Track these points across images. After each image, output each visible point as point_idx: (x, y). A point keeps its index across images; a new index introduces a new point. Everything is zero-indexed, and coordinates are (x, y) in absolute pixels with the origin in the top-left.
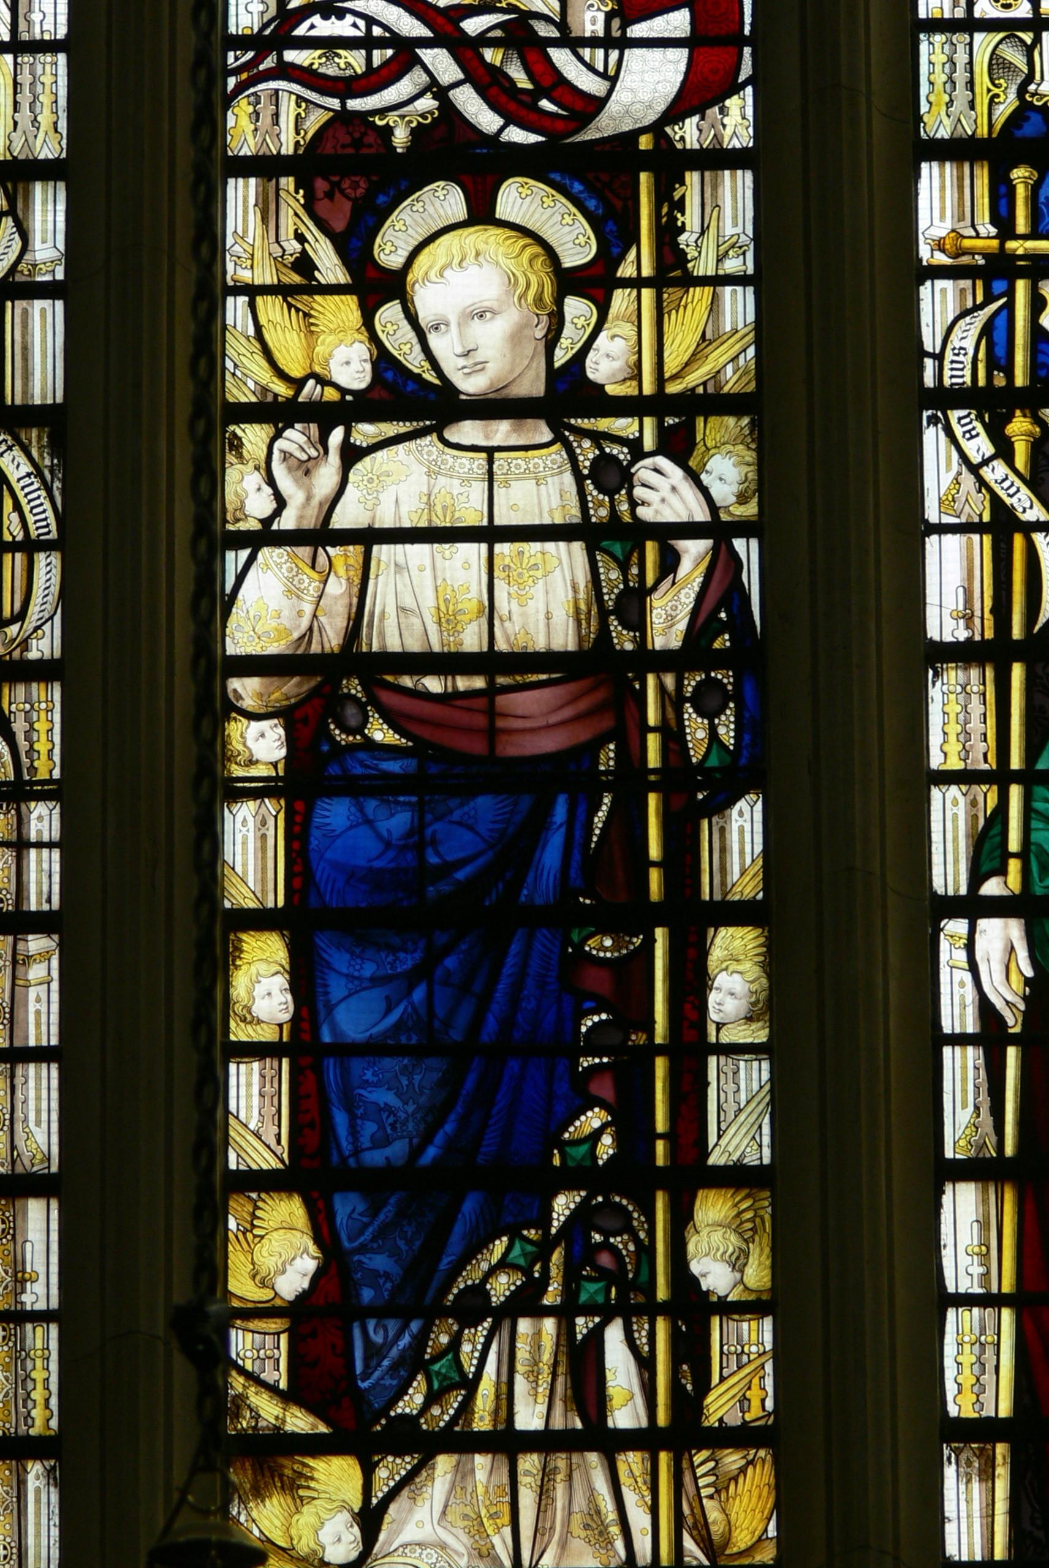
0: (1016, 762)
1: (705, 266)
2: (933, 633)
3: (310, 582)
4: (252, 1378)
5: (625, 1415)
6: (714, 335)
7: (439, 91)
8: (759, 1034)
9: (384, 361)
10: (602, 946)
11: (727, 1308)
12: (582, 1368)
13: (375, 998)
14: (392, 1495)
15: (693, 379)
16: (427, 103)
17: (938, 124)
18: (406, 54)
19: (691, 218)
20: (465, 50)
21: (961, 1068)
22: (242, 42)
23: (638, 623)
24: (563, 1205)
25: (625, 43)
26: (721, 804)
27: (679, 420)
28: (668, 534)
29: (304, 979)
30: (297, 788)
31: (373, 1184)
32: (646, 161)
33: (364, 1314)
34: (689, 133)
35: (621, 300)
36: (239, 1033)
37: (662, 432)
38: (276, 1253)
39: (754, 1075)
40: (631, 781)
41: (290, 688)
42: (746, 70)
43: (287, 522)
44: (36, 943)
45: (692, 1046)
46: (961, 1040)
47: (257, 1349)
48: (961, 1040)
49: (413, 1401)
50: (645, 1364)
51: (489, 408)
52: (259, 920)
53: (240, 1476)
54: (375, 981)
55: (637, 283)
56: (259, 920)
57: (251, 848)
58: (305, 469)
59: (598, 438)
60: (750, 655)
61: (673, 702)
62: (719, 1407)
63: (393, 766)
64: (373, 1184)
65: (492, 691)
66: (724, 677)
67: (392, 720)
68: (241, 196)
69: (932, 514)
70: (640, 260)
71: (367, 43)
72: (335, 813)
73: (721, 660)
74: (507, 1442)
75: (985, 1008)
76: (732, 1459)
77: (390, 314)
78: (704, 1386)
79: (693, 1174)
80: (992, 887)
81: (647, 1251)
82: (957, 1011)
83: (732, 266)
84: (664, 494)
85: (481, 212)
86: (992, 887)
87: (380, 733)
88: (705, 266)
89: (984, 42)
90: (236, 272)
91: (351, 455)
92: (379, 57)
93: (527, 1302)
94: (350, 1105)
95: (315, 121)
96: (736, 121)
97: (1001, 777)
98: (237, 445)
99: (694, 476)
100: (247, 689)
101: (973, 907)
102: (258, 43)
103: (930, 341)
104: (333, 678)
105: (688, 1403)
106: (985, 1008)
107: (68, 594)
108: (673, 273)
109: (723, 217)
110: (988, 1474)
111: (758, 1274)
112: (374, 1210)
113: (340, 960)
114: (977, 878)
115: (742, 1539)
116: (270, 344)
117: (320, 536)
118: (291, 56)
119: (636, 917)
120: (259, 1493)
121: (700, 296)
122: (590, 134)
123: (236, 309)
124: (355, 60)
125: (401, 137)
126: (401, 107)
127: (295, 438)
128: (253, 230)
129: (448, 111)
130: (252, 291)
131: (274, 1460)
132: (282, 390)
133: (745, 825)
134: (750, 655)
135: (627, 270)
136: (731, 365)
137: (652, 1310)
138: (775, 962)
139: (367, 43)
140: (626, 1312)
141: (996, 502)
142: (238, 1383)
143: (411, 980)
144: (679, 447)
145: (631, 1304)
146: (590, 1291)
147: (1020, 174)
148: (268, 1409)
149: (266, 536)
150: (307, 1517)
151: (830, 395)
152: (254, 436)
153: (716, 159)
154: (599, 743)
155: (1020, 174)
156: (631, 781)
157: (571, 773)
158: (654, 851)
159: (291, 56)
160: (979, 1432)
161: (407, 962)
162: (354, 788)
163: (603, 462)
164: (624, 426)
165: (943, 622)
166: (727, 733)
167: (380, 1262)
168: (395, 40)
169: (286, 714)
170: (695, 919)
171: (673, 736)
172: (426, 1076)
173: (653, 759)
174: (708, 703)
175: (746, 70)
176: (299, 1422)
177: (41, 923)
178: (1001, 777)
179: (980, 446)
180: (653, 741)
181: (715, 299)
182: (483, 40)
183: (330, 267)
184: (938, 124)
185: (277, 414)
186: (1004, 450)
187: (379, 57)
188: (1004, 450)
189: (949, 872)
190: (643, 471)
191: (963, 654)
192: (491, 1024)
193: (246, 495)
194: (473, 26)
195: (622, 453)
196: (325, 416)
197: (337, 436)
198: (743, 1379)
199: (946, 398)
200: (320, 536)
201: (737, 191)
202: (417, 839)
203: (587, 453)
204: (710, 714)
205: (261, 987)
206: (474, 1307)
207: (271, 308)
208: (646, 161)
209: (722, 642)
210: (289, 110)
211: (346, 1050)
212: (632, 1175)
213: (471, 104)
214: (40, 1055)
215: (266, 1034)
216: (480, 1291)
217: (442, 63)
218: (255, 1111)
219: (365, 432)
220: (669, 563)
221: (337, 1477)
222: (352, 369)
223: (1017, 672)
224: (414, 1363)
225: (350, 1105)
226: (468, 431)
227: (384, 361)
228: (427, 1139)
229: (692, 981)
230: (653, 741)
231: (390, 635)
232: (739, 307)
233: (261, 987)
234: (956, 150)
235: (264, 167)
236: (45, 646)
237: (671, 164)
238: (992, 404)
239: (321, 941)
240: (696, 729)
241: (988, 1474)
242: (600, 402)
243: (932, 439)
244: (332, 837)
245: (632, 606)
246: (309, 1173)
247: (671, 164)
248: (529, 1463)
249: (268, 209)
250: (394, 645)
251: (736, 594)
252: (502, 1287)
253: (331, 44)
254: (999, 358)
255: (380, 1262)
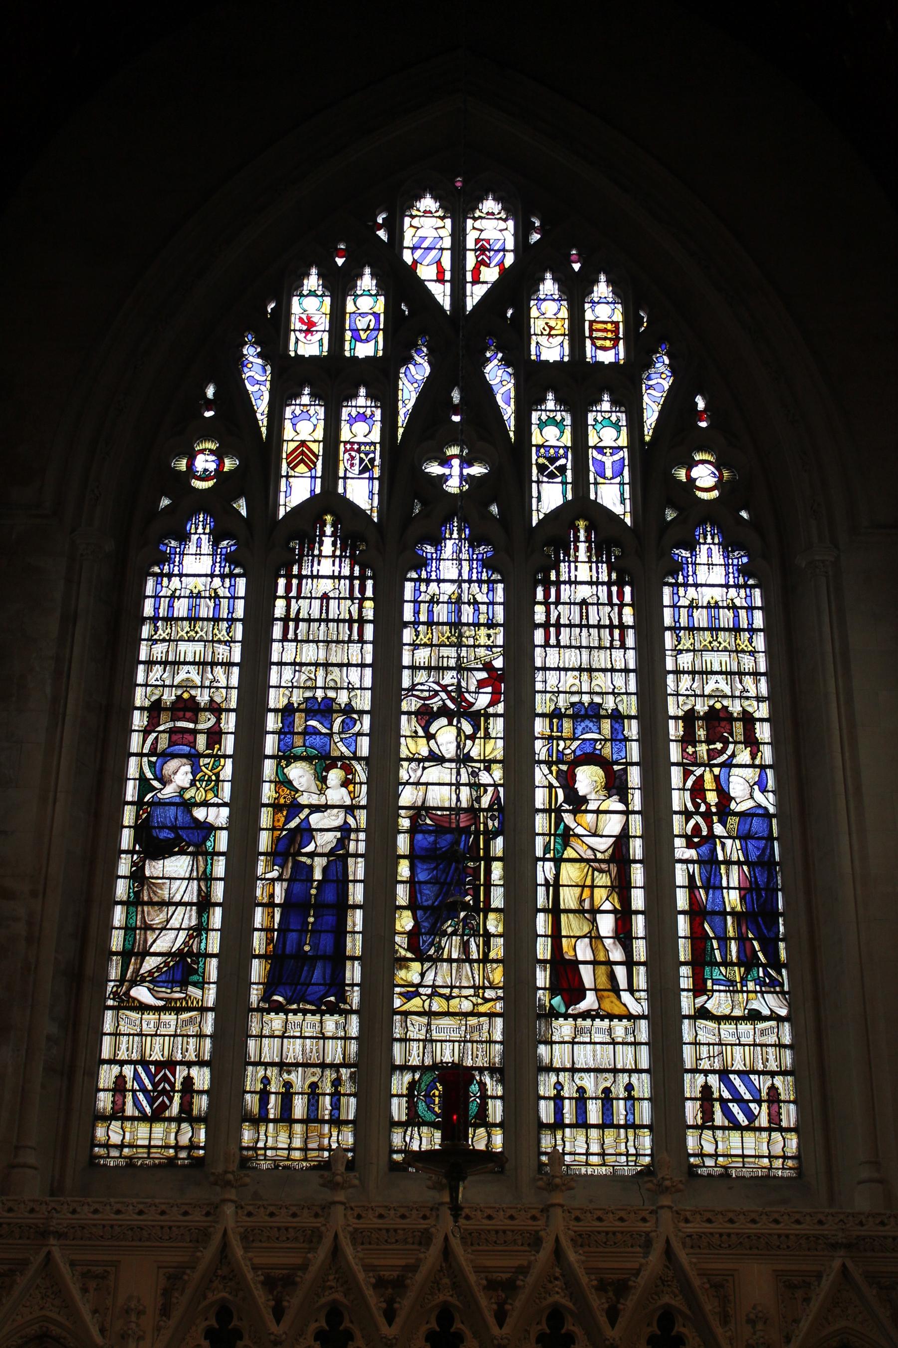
0: (553, 832)
1: (493, 735)
2: (537, 806)
3: (415, 792)
4: (400, 946)
5: (475, 956)
6: (496, 749)
7: (443, 701)
8: (501, 882)
9: (431, 751)
10: (471, 864)
11: (494, 936)
12: (465, 946)
13: (427, 872)
14: (427, 970)
15: (491, 757)
16: (441, 702)
17: (539, 710)
18: (436, 693)
19: (491, 726)
20: (448, 693)
21: (541, 891)
22: (405, 690)
23: (479, 803)
24: (462, 914)
25: (479, 693)
26: (495, 838)
27: (488, 764)
28: (485, 786)
29: (412, 868)
30: (413, 831)
31: (425, 909)
32: (483, 715)
33: (422, 934)
34: (491, 710)
35: (477, 741)
36: (399, 878)
37: (485, 767)
38: (405, 922)
39: (501, 890)
40: (477, 833)
41: (411, 812)
42: (502, 699)
43: (411, 781)
44: (360, 860)
45: (488, 885)
46: (541, 885)
47: (401, 941)
48: (541, 885)
49: (432, 952)
50: (478, 946)
51: (450, 761)
52: (404, 857)
53: (397, 966)
54: (426, 869)
55: (480, 738)
56: (404, 857)
57: (403, 843)
58: (415, 771)
59: (472, 767)
60: (501, 809)
61: (486, 818)
62: (492, 955)
63: (431, 828)
64: (425, 909)
65: (450, 814)
66: (496, 814)
67: (431, 819)
68: (404, 718)
69: (537, 784)
70: (481, 734)
71: (429, 691)
72: (419, 837)
73: (495, 810)
74: (450, 960)
75: (546, 879)
76: (495, 965)
77: (432, 742)
78: (489, 951)
79: (488, 909)
80: (547, 856)
81: (478, 924)
82: (540, 880)
83: (499, 736)
84: (485, 778)
85: (450, 724)
86: (547, 856)
87: (428, 821)
88: (493, 735)
89: (548, 695)
90: (403, 733)
91: (424, 768)
92: (431, 693)
93: (454, 933)
94: (421, 893)
95: (419, 705)
96: (500, 708)
97: (550, 835)
98: (402, 766)
99: (491, 775)
100: (402, 812)
101: (544, 860)
102: (408, 690)
103: (537, 751)
104: (419, 811)
105: (486, 955)
106: (546, 879)
107: (368, 793)
108: (487, 736)
109: (497, 727)
110: (545, 970)
111: (501, 929)
112: (425, 914)
113: (419, 865)
114: (545, 854)
115: (496, 982)
116: (407, 747)
117: (417, 783)
118: (414, 693)
119: (479, 859)
120: (401, 969)
121: (493, 741)
122: (472, 710)
123: (402, 740)
124: (426, 694)
125: (435, 709)
126: (435, 704)
127: (413, 765)
128: (406, 725)
129: (444, 704)
130: (406, 737)
131: (403, 962)
132: (411, 756)
133: (500, 841)
134: (501, 809)
135: (478, 735)
136: (499, 754)
137: (479, 936)
138: (504, 869)
139: (429, 691)
140: (474, 936)
141: (549, 782)
142: (397, 947)
143: (433, 869)
144: (488, 769)
145: (476, 934)
146: (467, 931)
147: (555, 720)
148: (403, 952)
149: (407, 783)
150: (410, 974)
151: (518, 760)
152: (405, 764)
153: (496, 715)
154: (471, 825)
155: (555, 720)
156: (477, 833)
157: (466, 831)
158: (482, 846)
159: (414, 693)
160: (544, 962)
161: (432, 866)
162: (423, 832)
163: (473, 772)
164: (477, 765)
165: (539, 805)
166: (496, 824)
167: (426, 924)
168: (434, 690)
169: (410, 818)
170: (489, 860)
171: (486, 825)
172: (436, 888)
173: (482, 829)
174: (493, 818)
175: (502, 699)
176: (409, 955)
177: (361, 856)
178: (550, 835)
179: (546, 771)
180: (482, 825)
181: (495, 743)
182: (451, 691)
183: (421, 733)
184: (539, 710)
185: (409, 760)
186: (551, 772)
187: (431, 693)
188: (551, 772)
189: (539, 853)
190: (481, 773)
191: (543, 811)
192: (449, 878)
193: (403, 775)
194: (449, 688)
195: (477, 770)
196: (419, 761)
197: (421, 765)
198: (497, 949)
199: (540, 762)
200: (417, 783)
201: (500, 721)
202: (435, 842)
203: (470, 770)
204: (493, 821)
205: (404, 869)
206: (444, 934)
207: (409, 740)
208: (483, 715)
209: (496, 807)
210: (414, 703)
211: (420, 883)
212: (476, 909)
213: (449, 704)
214: (360, 881)
215: (405, 879)
216: (446, 931)
217: (443, 695)
218: (402, 894)
219: (427, 764)
220: (486, 791)
221: (416, 966)
222: (425, 753)
223: (553, 814)
224: (432, 944)
225: (421, 893)
226: (447, 765)
227: (431, 751)
228: (436, 900)
229: (488, 872)
230: (482, 825)
231: (431, 803)
232: (500, 743)
233: (404, 869)
234: (543, 715)
235: (409, 713)
236: (364, 802)
237: (487, 716)
238: (549, 764)
239: (416, 861)
240: (490, 823)
241: (545, 970)
242: (473, 760)
243: (537, 770)
244: (418, 841)
245: (478, 799)
246: (412, 906)
247: (487, 716)
248: (455, 965)
249: (409, 721)
250: (432, 805)
251: (498, 798)
252: (450, 930)
253: (422, 691)
254: (550, 755)
255: (426, 924)
